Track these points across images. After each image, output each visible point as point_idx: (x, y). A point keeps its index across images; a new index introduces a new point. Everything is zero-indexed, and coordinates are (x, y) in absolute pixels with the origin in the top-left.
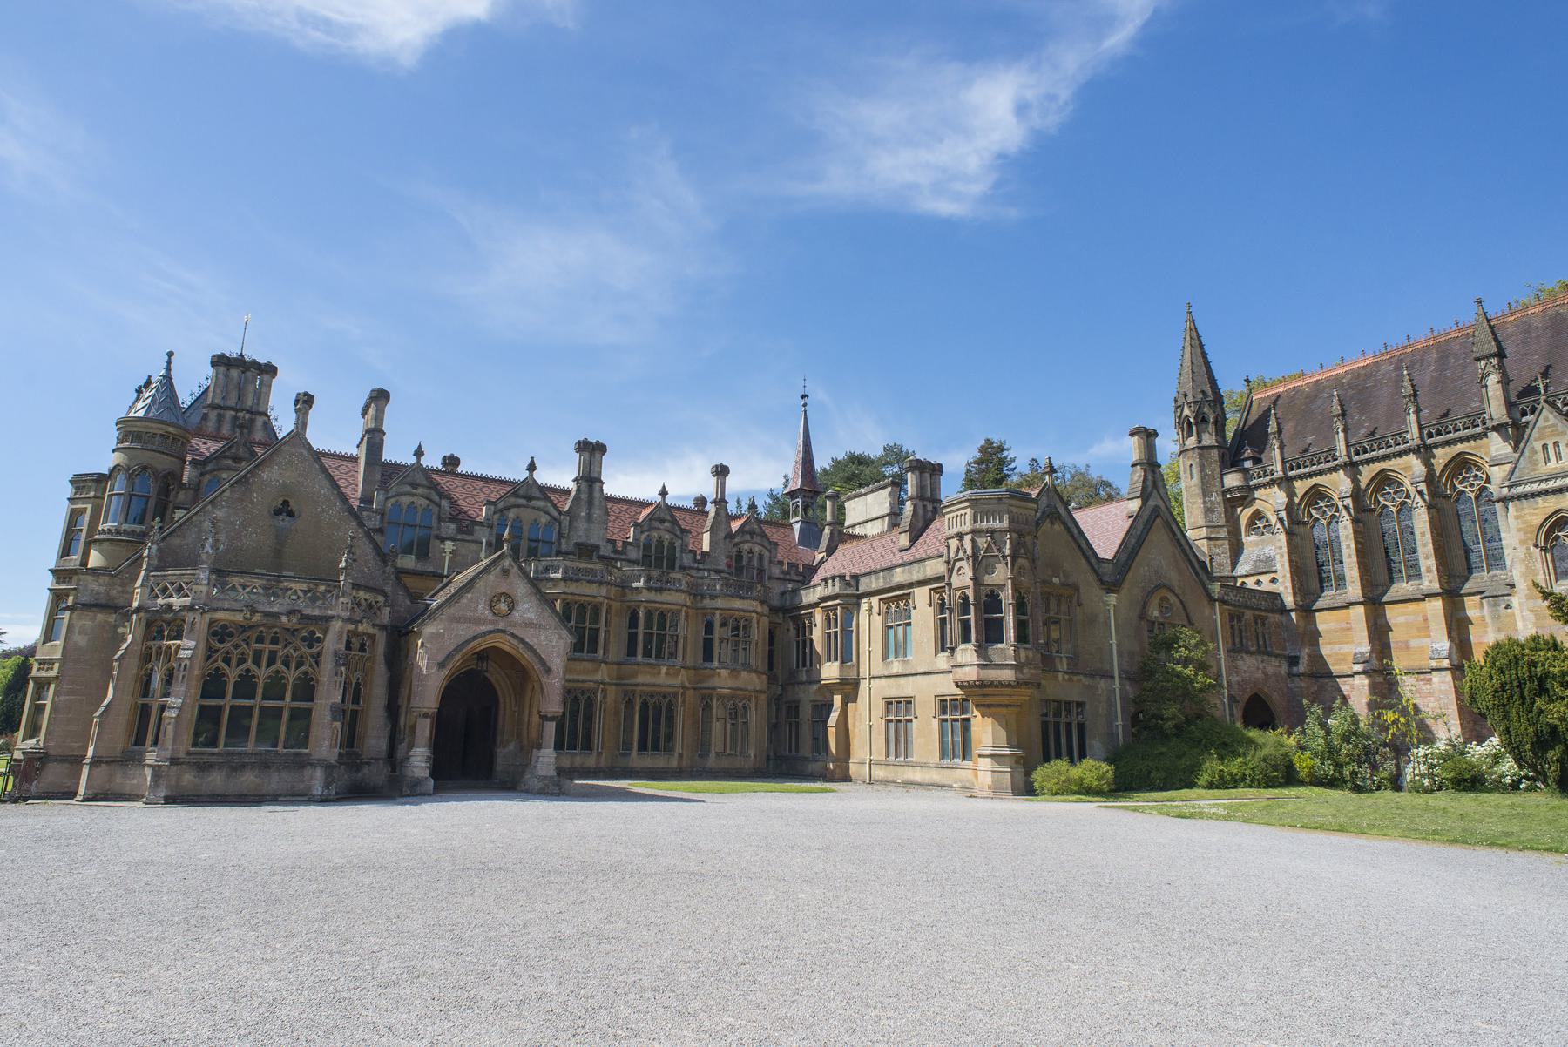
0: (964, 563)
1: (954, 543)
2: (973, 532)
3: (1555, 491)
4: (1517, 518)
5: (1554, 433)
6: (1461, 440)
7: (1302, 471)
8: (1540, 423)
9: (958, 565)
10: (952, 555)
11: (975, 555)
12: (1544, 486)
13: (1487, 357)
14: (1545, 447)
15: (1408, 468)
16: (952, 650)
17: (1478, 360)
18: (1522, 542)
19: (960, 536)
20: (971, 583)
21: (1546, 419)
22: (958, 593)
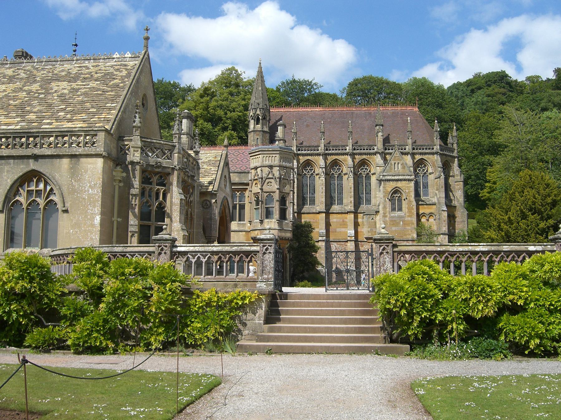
0: (272, 180)
1: (266, 170)
2: (279, 166)
3: (397, 180)
4: (384, 187)
5: (398, 160)
6: (365, 154)
7: (303, 152)
8: (395, 155)
9: (268, 181)
10: (264, 175)
11: (280, 178)
12: (393, 178)
13: (380, 125)
14: (395, 163)
15: (345, 160)
16: (262, 222)
17: (376, 125)
18: (384, 196)
19: (271, 167)
20: (278, 191)
21: (397, 154)
22: (266, 195)
